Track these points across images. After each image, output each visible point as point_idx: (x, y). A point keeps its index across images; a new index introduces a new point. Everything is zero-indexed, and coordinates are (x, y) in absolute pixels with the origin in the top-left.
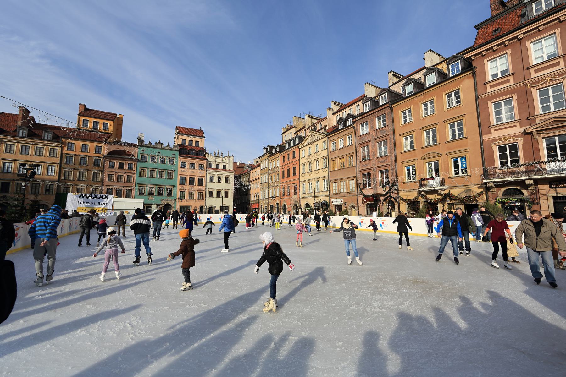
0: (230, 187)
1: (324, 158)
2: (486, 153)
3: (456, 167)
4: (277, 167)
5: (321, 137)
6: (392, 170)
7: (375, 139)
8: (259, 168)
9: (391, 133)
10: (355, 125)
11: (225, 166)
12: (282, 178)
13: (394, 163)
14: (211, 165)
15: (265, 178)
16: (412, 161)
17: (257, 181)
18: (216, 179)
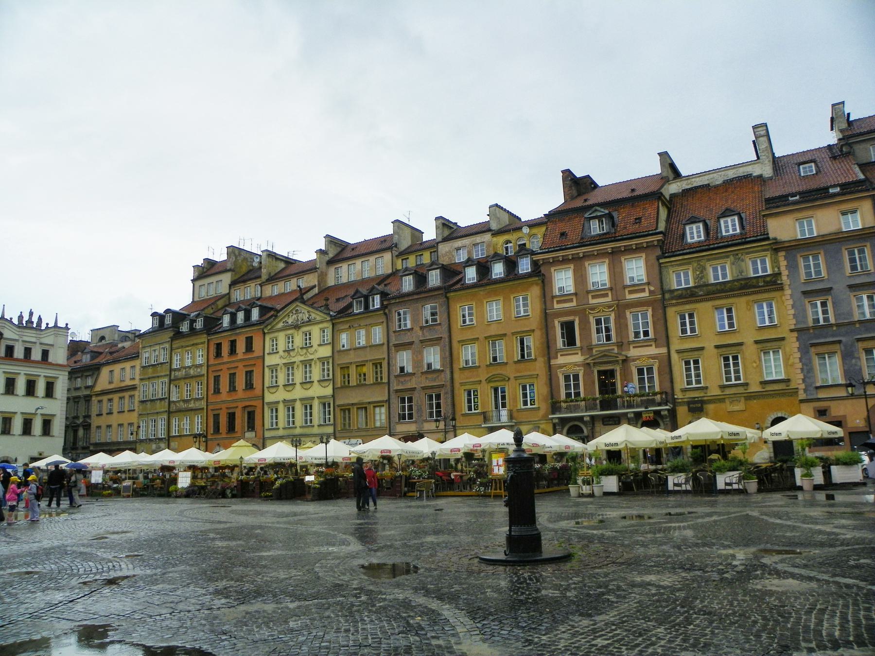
0: (57, 408)
1: (323, 360)
2: (553, 382)
3: (525, 395)
4: (201, 366)
5: (318, 318)
6: (446, 393)
7: (422, 341)
8: (137, 363)
9: (445, 335)
10: (387, 311)
11: (45, 354)
12: (212, 391)
13: (448, 384)
14: (10, 350)
15: (158, 388)
16: (474, 383)
17: (126, 395)
18: (21, 386)
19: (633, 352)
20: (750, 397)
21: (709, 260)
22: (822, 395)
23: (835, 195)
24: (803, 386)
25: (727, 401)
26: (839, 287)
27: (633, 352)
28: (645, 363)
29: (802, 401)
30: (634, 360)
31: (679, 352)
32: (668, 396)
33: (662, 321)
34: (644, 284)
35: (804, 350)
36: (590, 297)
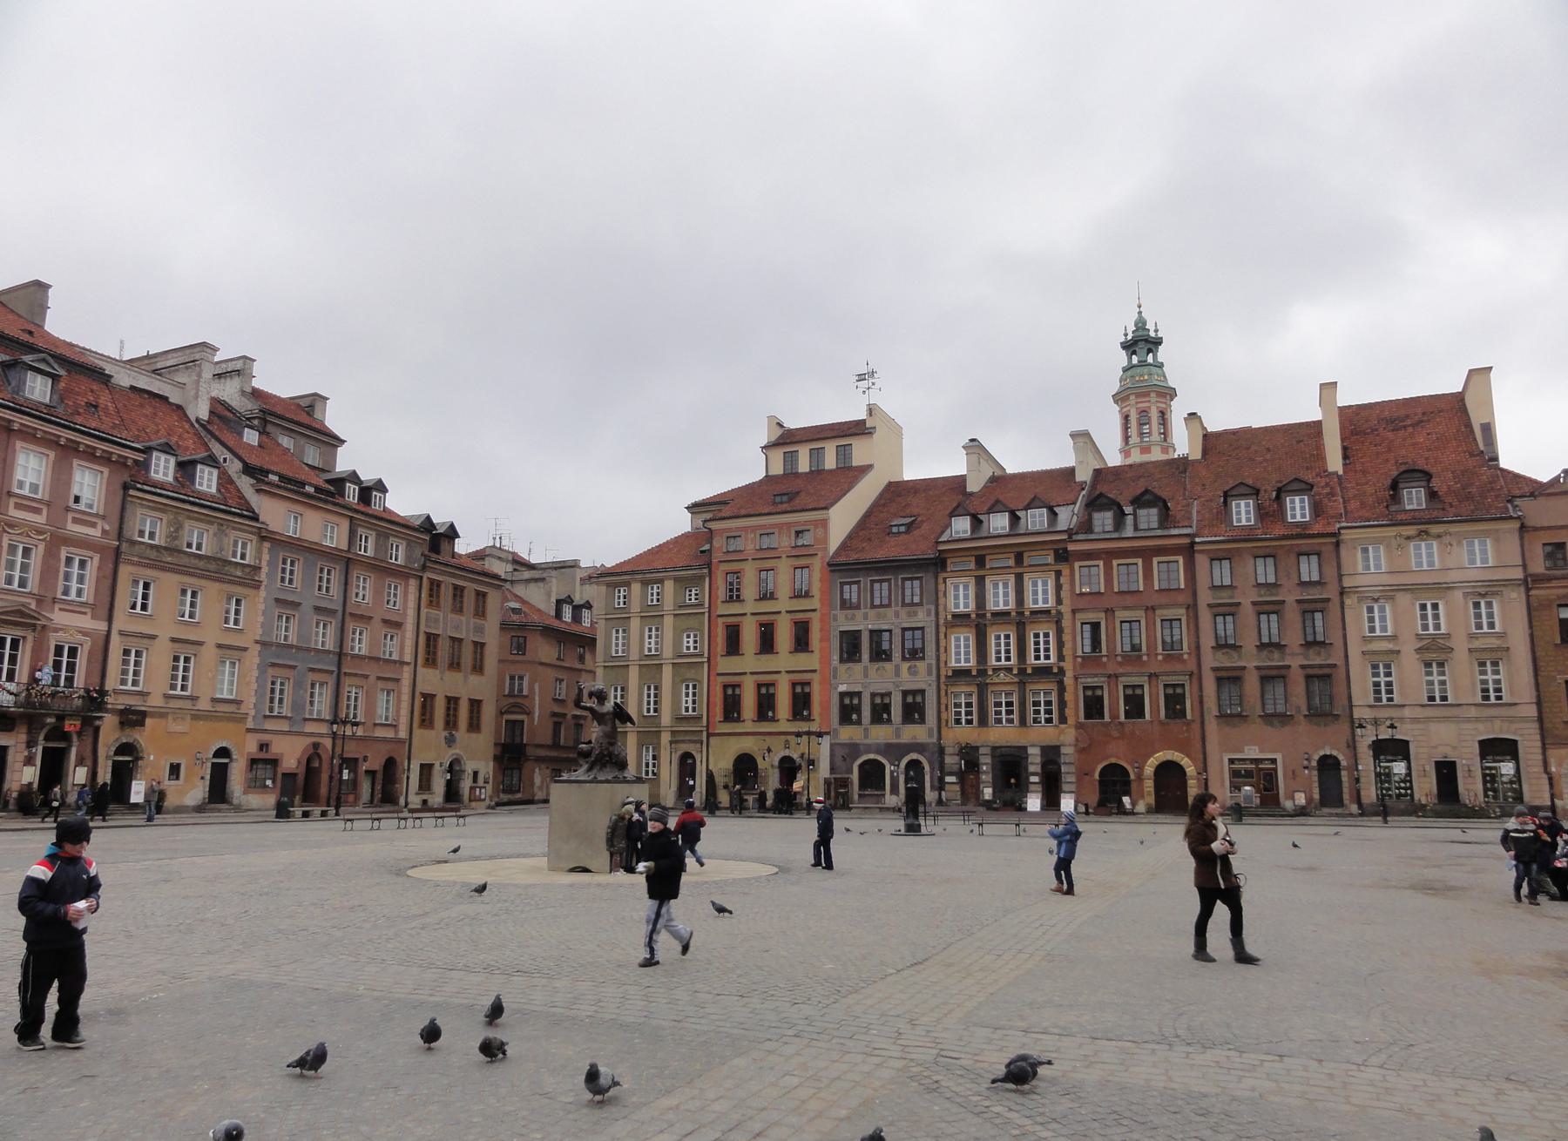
19: (58, 617)
20: (197, 716)
21: (189, 518)
22: (269, 725)
23: (308, 495)
24: (252, 713)
25: (170, 717)
26: (307, 606)
27: (58, 617)
28: (70, 639)
29: (249, 730)
30: (56, 630)
31: (121, 633)
32: (95, 701)
33: (108, 583)
34: (96, 515)
35: (262, 668)
36: (12, 505)
